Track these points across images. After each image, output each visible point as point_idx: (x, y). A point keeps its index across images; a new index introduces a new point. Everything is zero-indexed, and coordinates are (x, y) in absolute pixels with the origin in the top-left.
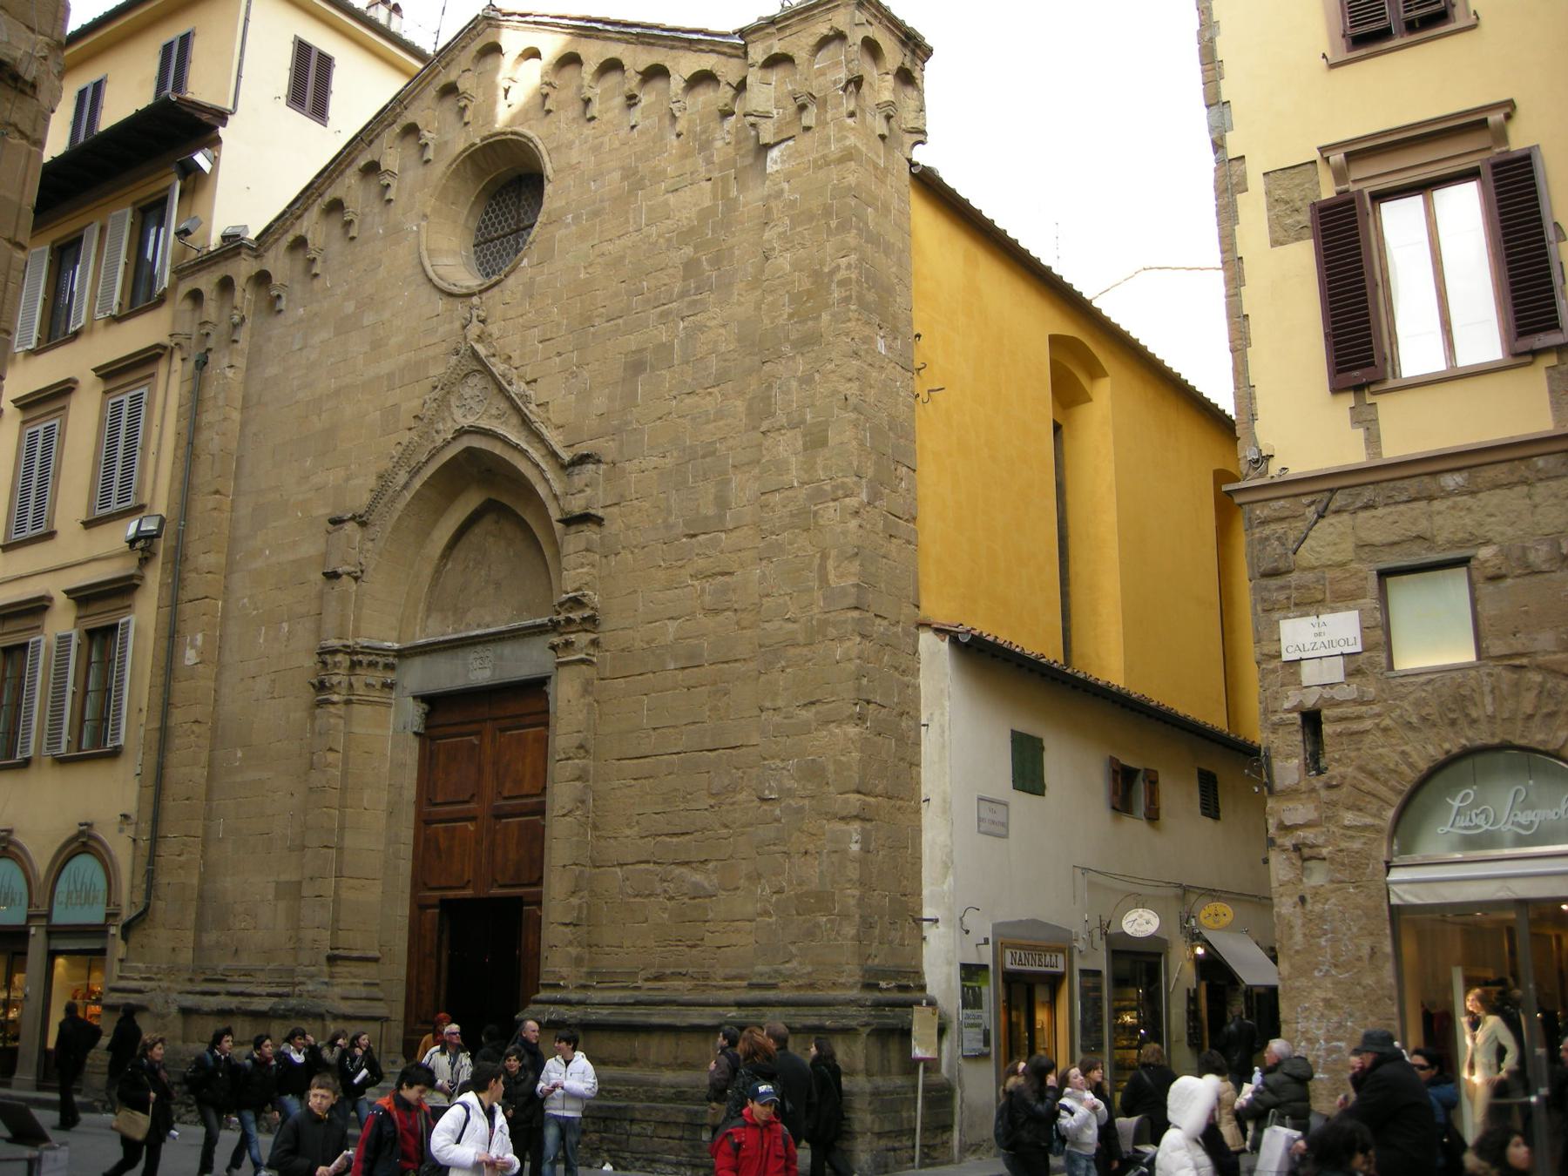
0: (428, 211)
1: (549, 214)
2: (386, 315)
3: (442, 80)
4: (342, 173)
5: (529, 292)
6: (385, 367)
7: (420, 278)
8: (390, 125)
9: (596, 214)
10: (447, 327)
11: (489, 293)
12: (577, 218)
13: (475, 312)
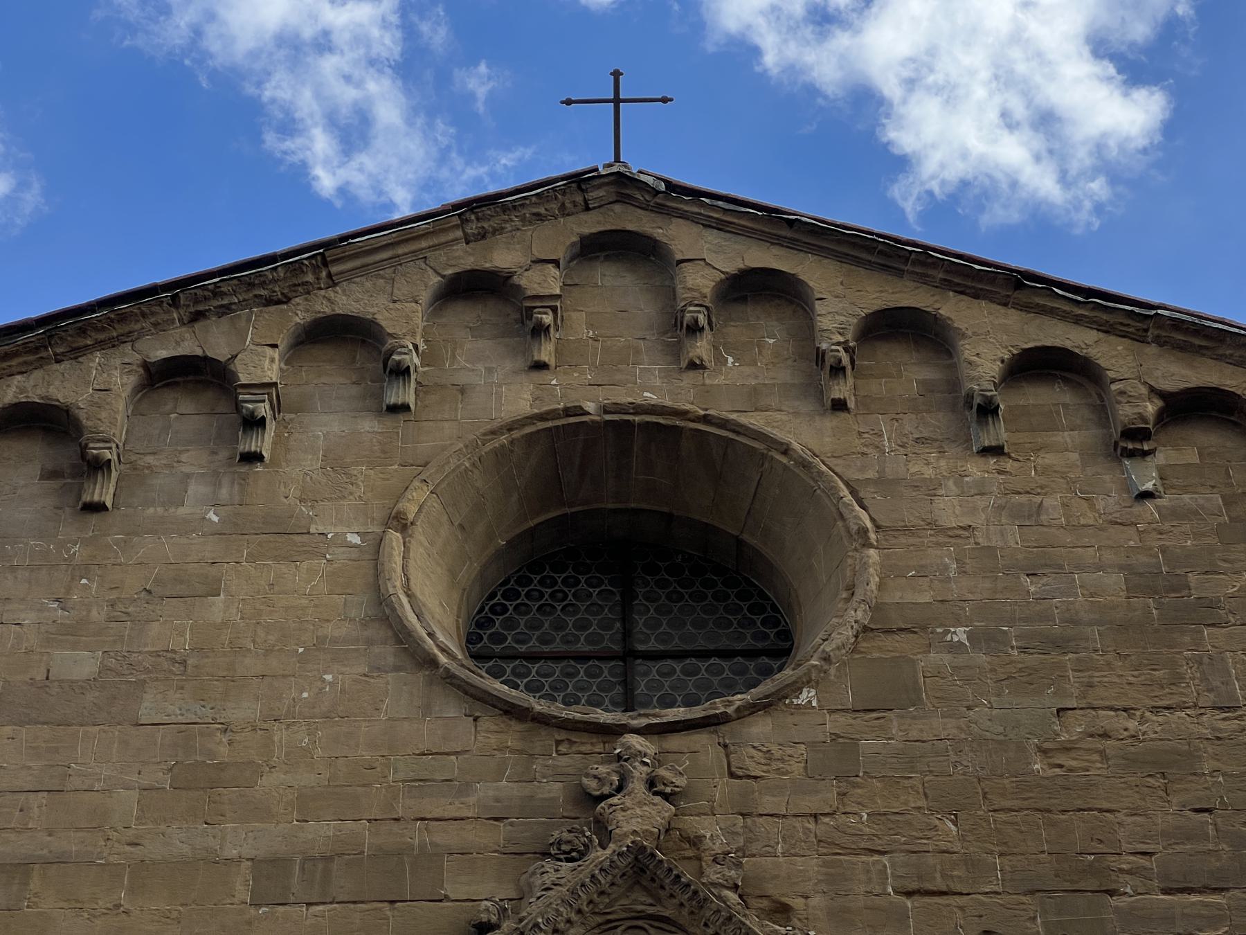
0: (411, 510)
1: (877, 609)
2: (243, 711)
3: (465, 259)
4: (76, 353)
5: (839, 762)
6: (240, 841)
7: (387, 653)
8: (269, 302)
9: (1060, 644)
10: (507, 788)
11: (674, 742)
12: (984, 639)
13: (639, 772)
